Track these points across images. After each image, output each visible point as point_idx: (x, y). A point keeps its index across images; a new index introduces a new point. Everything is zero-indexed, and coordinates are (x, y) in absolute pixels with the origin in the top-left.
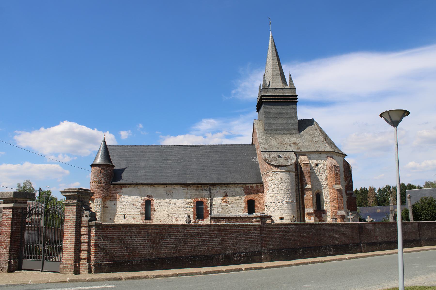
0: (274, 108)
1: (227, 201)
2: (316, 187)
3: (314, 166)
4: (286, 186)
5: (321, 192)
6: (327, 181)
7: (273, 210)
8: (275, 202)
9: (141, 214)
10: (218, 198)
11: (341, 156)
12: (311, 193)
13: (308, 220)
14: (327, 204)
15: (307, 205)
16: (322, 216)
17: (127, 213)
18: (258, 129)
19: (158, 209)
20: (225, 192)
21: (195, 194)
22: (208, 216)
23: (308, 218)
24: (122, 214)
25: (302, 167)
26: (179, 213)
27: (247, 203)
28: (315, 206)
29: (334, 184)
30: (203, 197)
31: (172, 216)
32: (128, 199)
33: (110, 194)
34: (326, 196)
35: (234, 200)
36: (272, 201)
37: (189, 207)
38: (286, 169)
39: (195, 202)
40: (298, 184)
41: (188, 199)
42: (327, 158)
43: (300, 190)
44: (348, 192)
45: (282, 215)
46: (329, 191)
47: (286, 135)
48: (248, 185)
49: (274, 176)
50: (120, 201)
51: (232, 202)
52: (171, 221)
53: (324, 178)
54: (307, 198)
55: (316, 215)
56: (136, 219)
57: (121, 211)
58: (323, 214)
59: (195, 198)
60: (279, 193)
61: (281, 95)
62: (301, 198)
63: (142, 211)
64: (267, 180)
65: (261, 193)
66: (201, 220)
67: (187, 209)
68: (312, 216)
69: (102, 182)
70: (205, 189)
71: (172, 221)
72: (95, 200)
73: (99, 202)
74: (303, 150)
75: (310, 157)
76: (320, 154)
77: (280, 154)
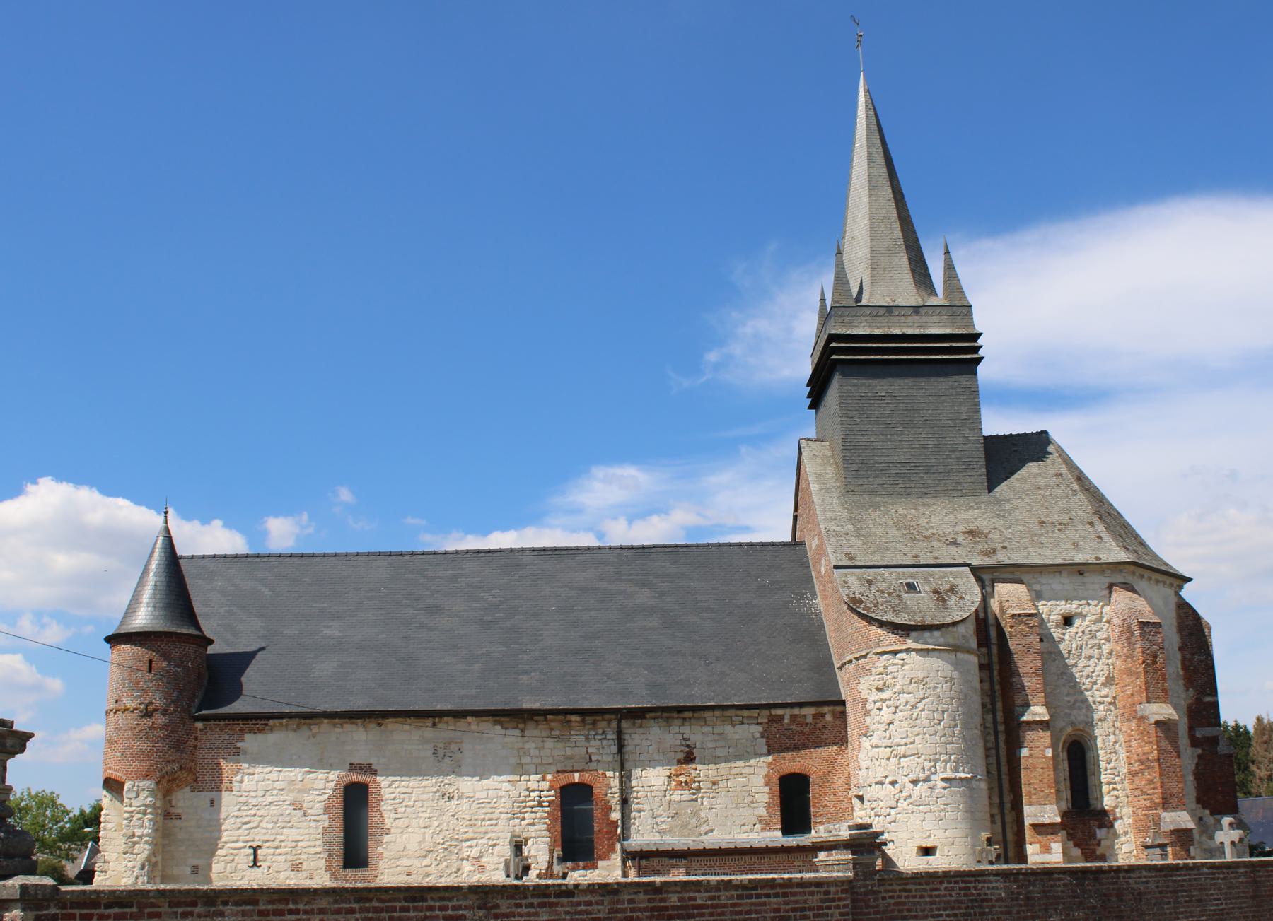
0: (881, 386)
1: (695, 782)
2: (1066, 714)
3: (1057, 626)
4: (943, 712)
5: (1088, 733)
6: (1114, 687)
7: (889, 815)
8: (899, 781)
9: (327, 844)
10: (654, 768)
11: (1165, 583)
12: (1048, 741)
13: (1036, 856)
14: (1115, 783)
16: (1094, 836)
17: (267, 841)
18: (819, 477)
19: (400, 823)
20: (683, 742)
21: (556, 753)
22: (613, 850)
23: (1038, 845)
24: (245, 847)
25: (1007, 630)
26: (489, 836)
27: (777, 788)
28: (1067, 794)
29: (1144, 700)
30: (592, 766)
31: (460, 850)
32: (269, 782)
33: (193, 761)
34: (1111, 753)
35: (724, 777)
36: (886, 777)
37: (532, 812)
38: (942, 640)
39: (559, 791)
40: (993, 703)
41: (527, 777)
42: (1110, 593)
43: (1001, 728)
44: (1198, 735)
45: (929, 836)
46: (1124, 729)
47: (935, 499)
48: (779, 712)
49: (890, 669)
50: (234, 789)
51: (714, 783)
52: (456, 872)
53: (1099, 676)
54: (1031, 761)
55: (1071, 831)
56: (304, 867)
57: (240, 831)
58: (1100, 827)
59: (558, 772)
60: (911, 743)
61: (910, 332)
62: (1003, 761)
63: (328, 830)
64: (860, 687)
65: (835, 744)
66: (581, 864)
67: (524, 819)
68: (1053, 836)
69: (156, 710)
70: (600, 731)
71: (460, 872)
72: (128, 785)
73: (143, 794)
74: (1007, 562)
75: (1037, 587)
76: (1081, 574)
77: (912, 576)
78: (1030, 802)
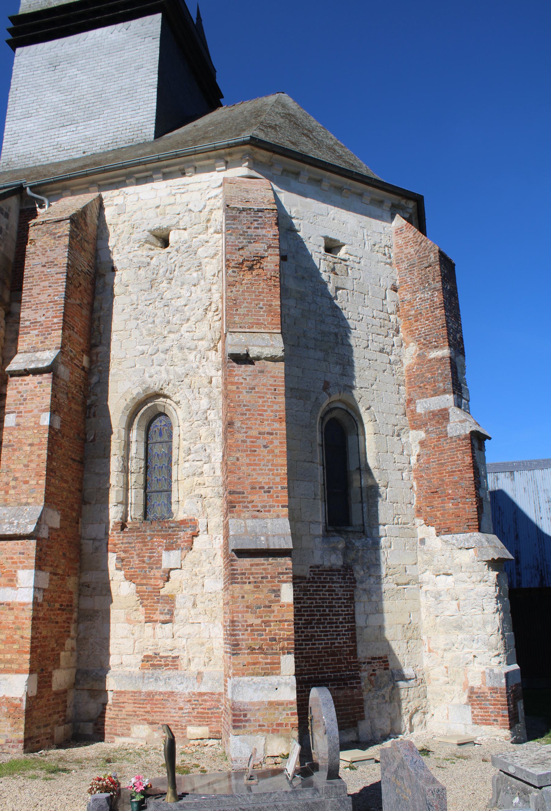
15: (12, 483)
16: (159, 561)
54: (15, 433)
55: (123, 555)
78: (6, 500)
